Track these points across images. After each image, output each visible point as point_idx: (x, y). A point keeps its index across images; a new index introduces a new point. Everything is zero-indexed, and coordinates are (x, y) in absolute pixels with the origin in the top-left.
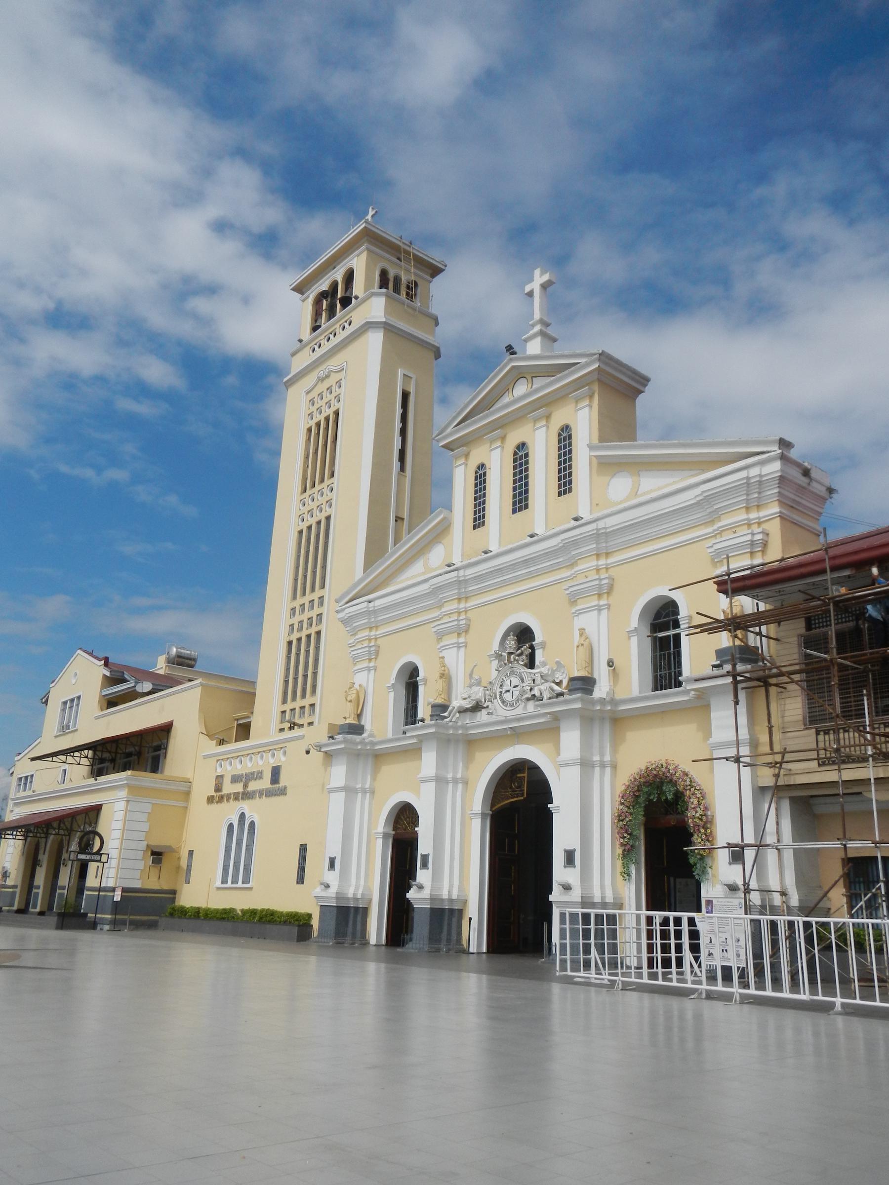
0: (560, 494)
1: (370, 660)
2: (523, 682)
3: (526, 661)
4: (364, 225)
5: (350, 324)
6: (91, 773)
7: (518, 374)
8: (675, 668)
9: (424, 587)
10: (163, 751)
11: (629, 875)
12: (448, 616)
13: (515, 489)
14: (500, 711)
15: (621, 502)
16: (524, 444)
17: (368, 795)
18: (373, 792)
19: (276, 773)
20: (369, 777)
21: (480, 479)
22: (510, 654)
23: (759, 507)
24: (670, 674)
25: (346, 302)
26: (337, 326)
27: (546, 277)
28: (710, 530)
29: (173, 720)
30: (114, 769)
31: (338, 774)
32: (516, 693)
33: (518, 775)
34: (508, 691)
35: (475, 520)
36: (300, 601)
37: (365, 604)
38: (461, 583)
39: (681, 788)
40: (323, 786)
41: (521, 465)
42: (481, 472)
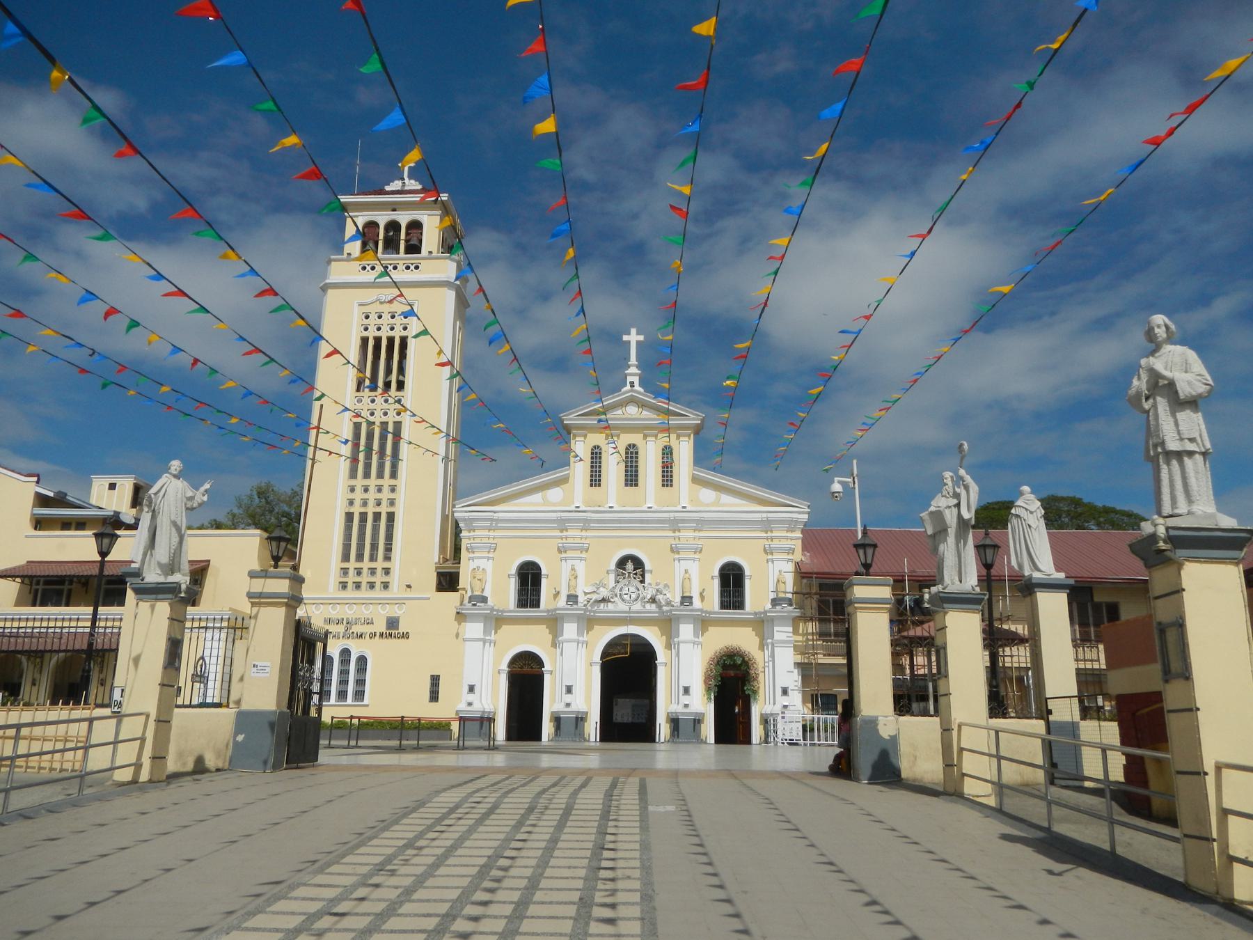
0: (663, 485)
1: (489, 552)
2: (638, 590)
3: (641, 579)
5: (417, 268)
6: (30, 593)
7: (632, 401)
9: (554, 515)
11: (710, 699)
12: (572, 539)
14: (622, 607)
15: (707, 505)
16: (634, 445)
17: (492, 645)
18: (495, 643)
19: (392, 623)
20: (493, 631)
21: (596, 454)
22: (629, 573)
23: (792, 531)
24: (730, 601)
25: (414, 248)
26: (401, 262)
27: (641, 338)
28: (764, 535)
29: (209, 561)
30: (86, 592)
31: (474, 629)
32: (634, 596)
35: (591, 480)
36: (360, 482)
38: (586, 521)
39: (746, 659)
40: (457, 635)
41: (632, 458)
42: (598, 451)
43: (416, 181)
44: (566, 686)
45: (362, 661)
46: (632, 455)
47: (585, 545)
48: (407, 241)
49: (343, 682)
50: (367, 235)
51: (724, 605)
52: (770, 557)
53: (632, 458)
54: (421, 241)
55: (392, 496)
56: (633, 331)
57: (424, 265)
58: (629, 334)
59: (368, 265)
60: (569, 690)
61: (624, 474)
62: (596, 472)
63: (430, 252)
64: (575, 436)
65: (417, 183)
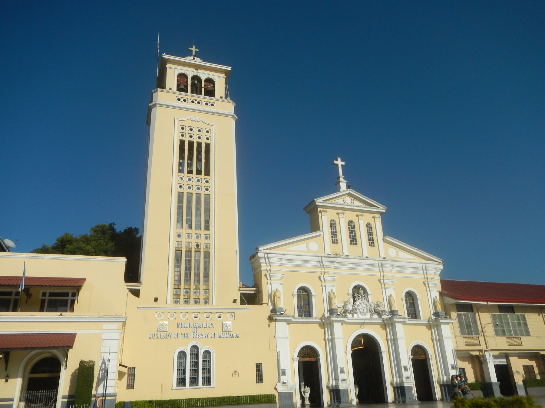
0: (370, 245)
2: (367, 306)
4: (230, 69)
8: (410, 311)
10: (70, 298)
13: (350, 236)
14: (361, 316)
21: (333, 226)
25: (210, 93)
26: (203, 100)
27: (343, 163)
32: (365, 310)
33: (359, 339)
34: (361, 309)
35: (332, 240)
37: (282, 256)
43: (201, 59)
44: (340, 368)
45: (207, 353)
46: (351, 226)
47: (336, 278)
48: (205, 89)
49: (194, 371)
50: (179, 81)
51: (408, 317)
52: (428, 289)
53: (352, 228)
54: (214, 90)
55: (206, 241)
56: (339, 159)
57: (217, 104)
58: (337, 160)
59: (182, 98)
60: (342, 371)
61: (349, 237)
62: (334, 235)
63: (221, 98)
64: (320, 212)
65: (202, 60)
